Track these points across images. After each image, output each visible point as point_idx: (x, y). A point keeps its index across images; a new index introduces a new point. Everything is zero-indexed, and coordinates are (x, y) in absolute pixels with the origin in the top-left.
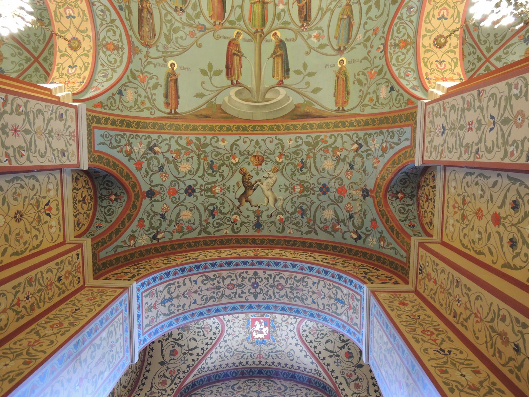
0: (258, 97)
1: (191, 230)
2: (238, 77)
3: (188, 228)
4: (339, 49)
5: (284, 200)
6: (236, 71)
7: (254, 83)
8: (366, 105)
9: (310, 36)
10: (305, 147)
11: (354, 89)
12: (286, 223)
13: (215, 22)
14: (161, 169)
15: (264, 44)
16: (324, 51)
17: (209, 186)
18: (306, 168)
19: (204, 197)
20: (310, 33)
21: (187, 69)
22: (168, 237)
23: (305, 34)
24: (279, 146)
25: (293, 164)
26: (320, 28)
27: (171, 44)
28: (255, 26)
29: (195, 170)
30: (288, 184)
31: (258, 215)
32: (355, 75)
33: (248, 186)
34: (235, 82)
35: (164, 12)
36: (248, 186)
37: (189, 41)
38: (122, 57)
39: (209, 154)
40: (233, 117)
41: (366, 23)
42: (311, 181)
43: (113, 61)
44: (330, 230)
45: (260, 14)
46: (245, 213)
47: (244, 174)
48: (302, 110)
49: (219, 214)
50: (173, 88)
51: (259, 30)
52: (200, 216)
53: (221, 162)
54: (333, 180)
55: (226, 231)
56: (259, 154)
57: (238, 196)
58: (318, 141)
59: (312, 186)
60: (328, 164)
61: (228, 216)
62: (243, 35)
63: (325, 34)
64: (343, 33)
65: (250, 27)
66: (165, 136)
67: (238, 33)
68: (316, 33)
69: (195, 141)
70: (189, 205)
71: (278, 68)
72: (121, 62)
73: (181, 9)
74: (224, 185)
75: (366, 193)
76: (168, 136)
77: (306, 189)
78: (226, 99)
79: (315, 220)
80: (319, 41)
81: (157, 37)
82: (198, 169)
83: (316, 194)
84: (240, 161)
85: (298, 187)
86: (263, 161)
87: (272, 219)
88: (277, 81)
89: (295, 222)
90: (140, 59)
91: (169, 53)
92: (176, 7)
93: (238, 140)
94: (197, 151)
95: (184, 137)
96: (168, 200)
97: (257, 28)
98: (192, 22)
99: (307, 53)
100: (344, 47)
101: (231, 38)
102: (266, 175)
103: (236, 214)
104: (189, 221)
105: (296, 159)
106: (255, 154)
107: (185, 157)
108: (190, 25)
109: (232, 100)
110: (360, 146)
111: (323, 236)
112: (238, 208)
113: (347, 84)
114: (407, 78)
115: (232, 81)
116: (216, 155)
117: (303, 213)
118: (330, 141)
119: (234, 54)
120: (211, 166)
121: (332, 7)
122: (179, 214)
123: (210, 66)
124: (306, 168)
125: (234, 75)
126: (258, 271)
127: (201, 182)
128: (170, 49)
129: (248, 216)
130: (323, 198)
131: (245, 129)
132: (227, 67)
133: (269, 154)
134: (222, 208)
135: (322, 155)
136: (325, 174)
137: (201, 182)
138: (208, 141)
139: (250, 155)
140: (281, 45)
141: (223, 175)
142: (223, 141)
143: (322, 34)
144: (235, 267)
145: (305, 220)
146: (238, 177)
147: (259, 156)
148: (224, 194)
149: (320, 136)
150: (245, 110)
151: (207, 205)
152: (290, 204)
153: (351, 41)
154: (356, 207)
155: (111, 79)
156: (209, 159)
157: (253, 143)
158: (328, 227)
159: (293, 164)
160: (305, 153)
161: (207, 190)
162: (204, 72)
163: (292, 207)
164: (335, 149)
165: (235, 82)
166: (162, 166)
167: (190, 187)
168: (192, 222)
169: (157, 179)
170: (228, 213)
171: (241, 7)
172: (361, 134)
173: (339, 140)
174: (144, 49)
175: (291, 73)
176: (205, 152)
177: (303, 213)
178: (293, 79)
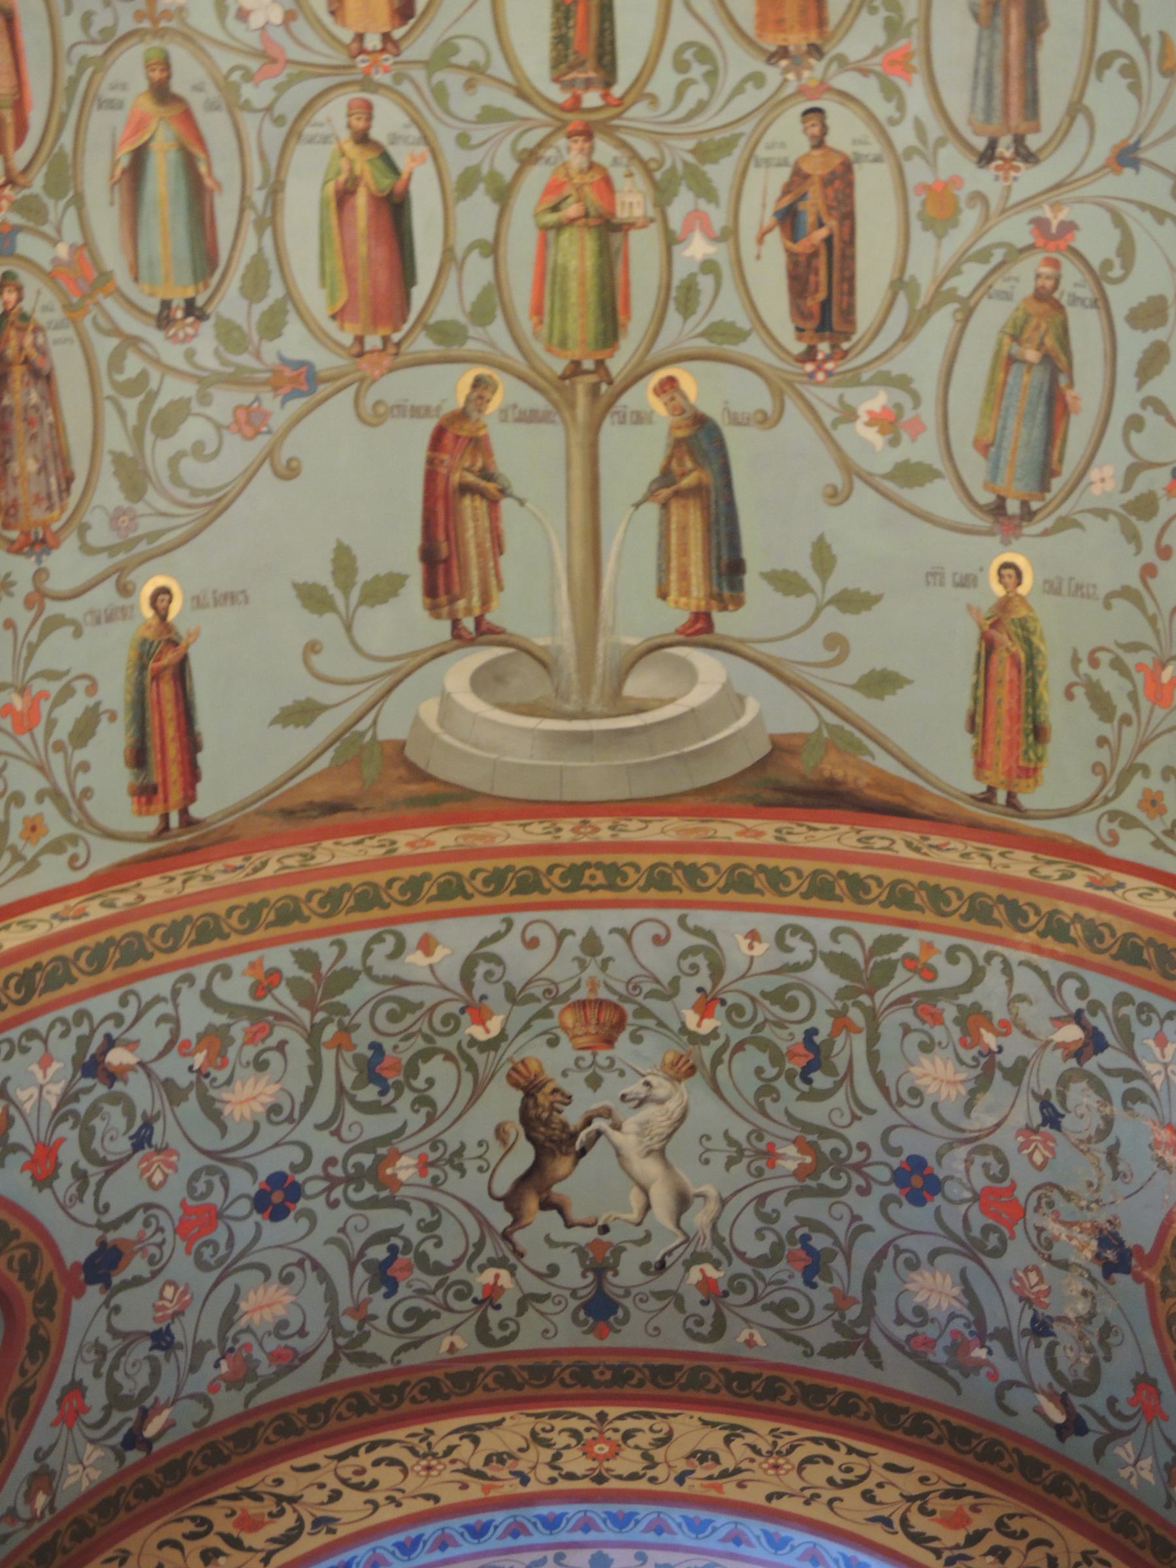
0: (586, 690)
1: (288, 1362)
2: (486, 601)
3: (274, 1356)
4: (998, 509)
5: (723, 1202)
6: (474, 575)
7: (566, 623)
8: (1129, 822)
9: (849, 415)
10: (825, 980)
11: (1070, 725)
12: (733, 1299)
13: (359, 340)
14: (141, 1140)
15: (610, 432)
16: (918, 496)
17: (367, 1160)
18: (831, 1071)
19: (344, 1210)
20: (851, 395)
21: (230, 598)
22: (188, 1416)
23: (824, 397)
24: (701, 960)
25: (765, 1045)
26: (903, 383)
27: (151, 495)
28: (563, 343)
29: (299, 1098)
30: (740, 1131)
31: (599, 1262)
32: (1075, 661)
33: (552, 1139)
34: (469, 623)
35: (104, 346)
36: (552, 1139)
37: (240, 453)
39: (363, 1018)
40: (465, 794)
41: (1135, 423)
42: (855, 1134)
44: (939, 1356)
45: (591, 283)
46: (539, 1258)
47: (530, 1087)
48: (807, 767)
49: (417, 1273)
50: (170, 710)
51: (588, 364)
52: (331, 1296)
53: (420, 1044)
54: (962, 1152)
55: (453, 1339)
56: (603, 994)
57: (503, 1186)
58: (891, 967)
59: (857, 1156)
60: (940, 1075)
61: (460, 1273)
62: (507, 392)
63: (928, 413)
64: (1021, 436)
65: (538, 348)
66: (147, 988)
67: (478, 383)
68: (878, 400)
69: (290, 969)
70: (276, 1261)
71: (684, 552)
73: (190, 307)
74: (434, 1144)
75: (1116, 1257)
76: (162, 984)
77: (826, 1165)
78: (429, 711)
79: (869, 1304)
80: (894, 442)
81: (77, 487)
82: (311, 1094)
83: (878, 1192)
84: (511, 1032)
85: (792, 1150)
86: (620, 1025)
87: (666, 1282)
88: (683, 617)
89: (777, 1297)
90: (9, 624)
91: (142, 547)
92: (166, 305)
93: (496, 937)
94: (304, 1015)
95: (239, 963)
96: (181, 1265)
97: (575, 352)
98: (246, 360)
99: (835, 497)
100: (1025, 504)
101: (447, 409)
102: (636, 1088)
103: (498, 1262)
104: (282, 1324)
105: (781, 1024)
106: (582, 994)
107: (250, 1052)
108: (237, 379)
109: (455, 712)
110: (1095, 1042)
111: (901, 1376)
112: (506, 1236)
113: (1033, 684)
115: (456, 623)
116: (393, 1017)
117: (815, 1266)
118: (951, 975)
119: (465, 489)
120: (372, 1068)
121: (964, 284)
122: (233, 1307)
123: (344, 562)
124: (831, 1071)
125: (465, 592)
126: (611, 1553)
127: (325, 1146)
128: (147, 525)
129: (554, 1270)
130: (907, 1214)
131: (529, 883)
132: (429, 556)
133: (651, 994)
134: (428, 1247)
135: (907, 1030)
136: (922, 1115)
137: (325, 1146)
138: (353, 959)
139: (556, 1000)
140: (701, 440)
141: (431, 1103)
142: (427, 945)
143: (909, 414)
144: (509, 1542)
145: (822, 1295)
146: (503, 1103)
147: (601, 1004)
148: (435, 1184)
149: (899, 941)
150: (522, 755)
151: (358, 1241)
152: (750, 1221)
153: (1056, 484)
154: (1070, 1297)
156: (362, 1039)
157: (572, 945)
158: (931, 1343)
159: (765, 1045)
160: (823, 1005)
161: (357, 1178)
162: (313, 598)
163: (759, 1234)
164: (973, 1019)
165: (469, 623)
166: (148, 1125)
167: (277, 1180)
168: (294, 1327)
169: (125, 1190)
170: (458, 1262)
171: (493, 249)
172: (1104, 988)
173: (994, 978)
175: (752, 581)
176: (343, 1010)
177: (815, 1266)
178: (758, 613)
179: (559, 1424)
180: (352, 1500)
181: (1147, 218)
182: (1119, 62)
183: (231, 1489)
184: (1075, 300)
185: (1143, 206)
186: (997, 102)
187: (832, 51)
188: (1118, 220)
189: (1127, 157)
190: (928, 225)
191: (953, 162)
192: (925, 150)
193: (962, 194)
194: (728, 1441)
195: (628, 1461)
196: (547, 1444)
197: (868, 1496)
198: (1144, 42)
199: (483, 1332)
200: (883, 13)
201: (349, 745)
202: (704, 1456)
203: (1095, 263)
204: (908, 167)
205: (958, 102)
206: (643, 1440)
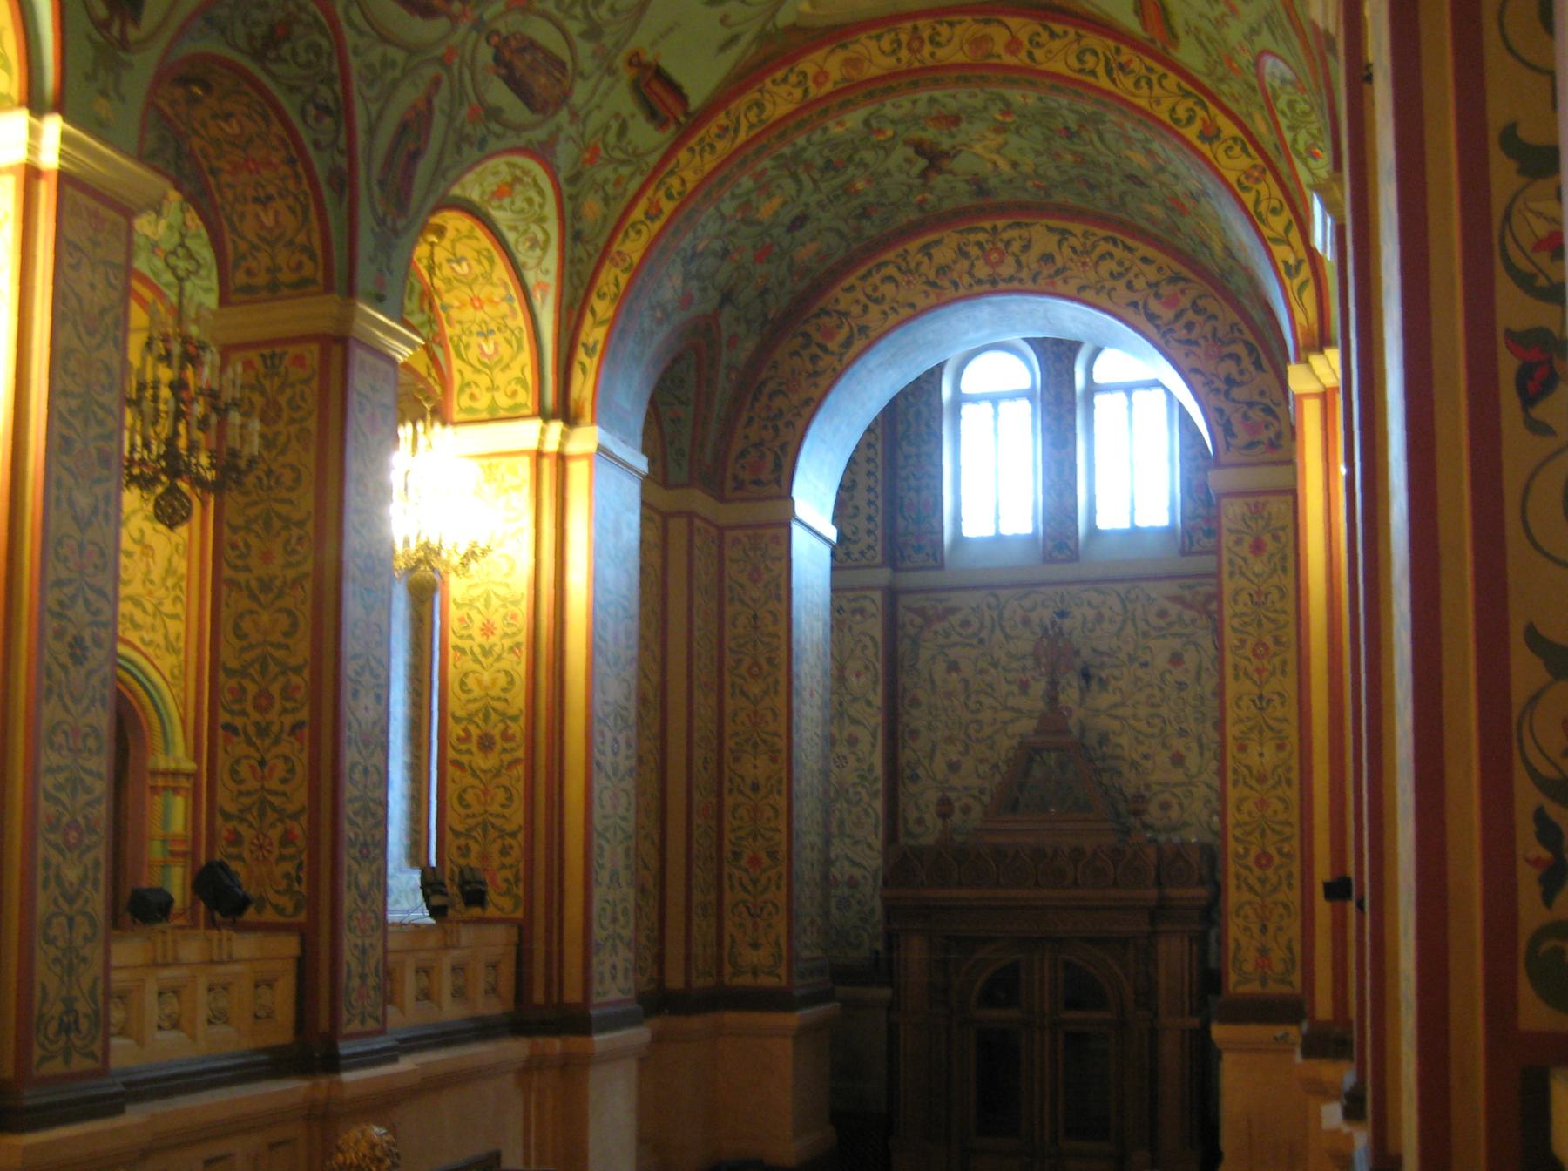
38: (536, 184)
43: (525, 205)
60: (1138, 157)
72: (541, 193)
114: (1311, 162)
142: (840, 124)
146: (902, 152)
155: (547, 241)
174: (563, 116)
179: (973, 238)
180: (874, 309)
183: (815, 310)
194: (1060, 243)
195: (1007, 269)
196: (965, 255)
197: (1130, 286)
199: (922, 210)
201: (764, 37)
202: (1047, 258)
206: (1016, 247)
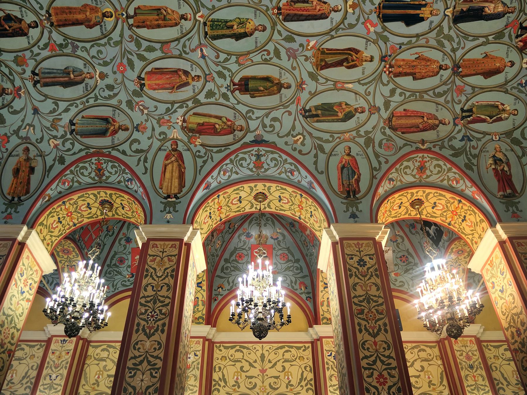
181: (23, 117)
182: (56, 107)
184: (3, 99)
185: (25, 116)
186: (47, 75)
187: (53, 29)
188: (22, 109)
189: (36, 111)
190: (16, 57)
191: (32, 64)
192: (34, 56)
193: (24, 67)
198: (60, 114)
200: (64, 43)
203: (12, 104)
204: (29, 51)
205: (45, 65)
